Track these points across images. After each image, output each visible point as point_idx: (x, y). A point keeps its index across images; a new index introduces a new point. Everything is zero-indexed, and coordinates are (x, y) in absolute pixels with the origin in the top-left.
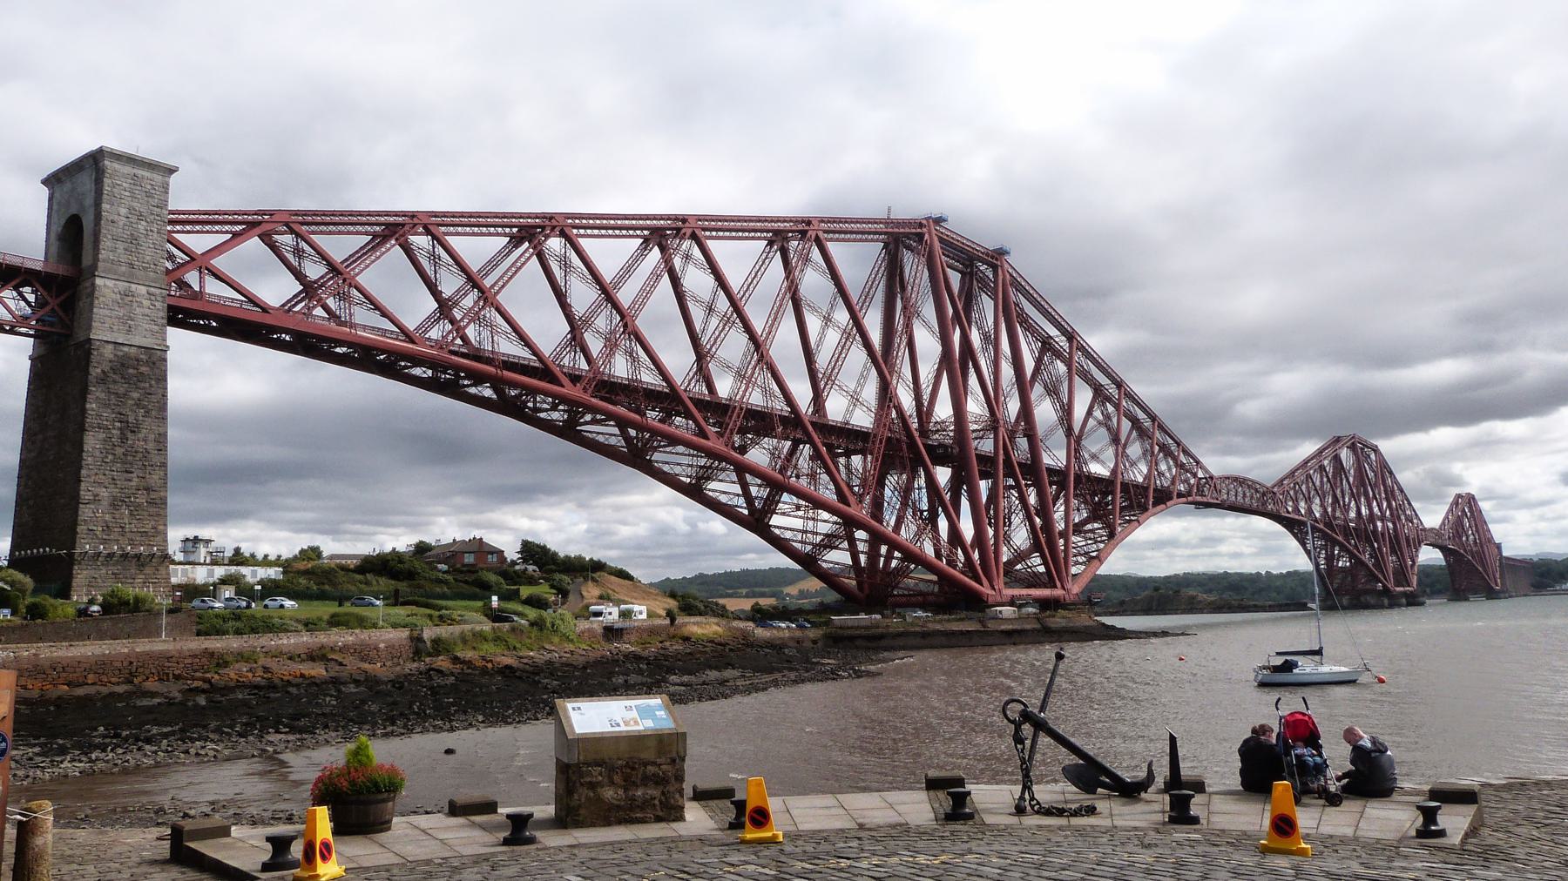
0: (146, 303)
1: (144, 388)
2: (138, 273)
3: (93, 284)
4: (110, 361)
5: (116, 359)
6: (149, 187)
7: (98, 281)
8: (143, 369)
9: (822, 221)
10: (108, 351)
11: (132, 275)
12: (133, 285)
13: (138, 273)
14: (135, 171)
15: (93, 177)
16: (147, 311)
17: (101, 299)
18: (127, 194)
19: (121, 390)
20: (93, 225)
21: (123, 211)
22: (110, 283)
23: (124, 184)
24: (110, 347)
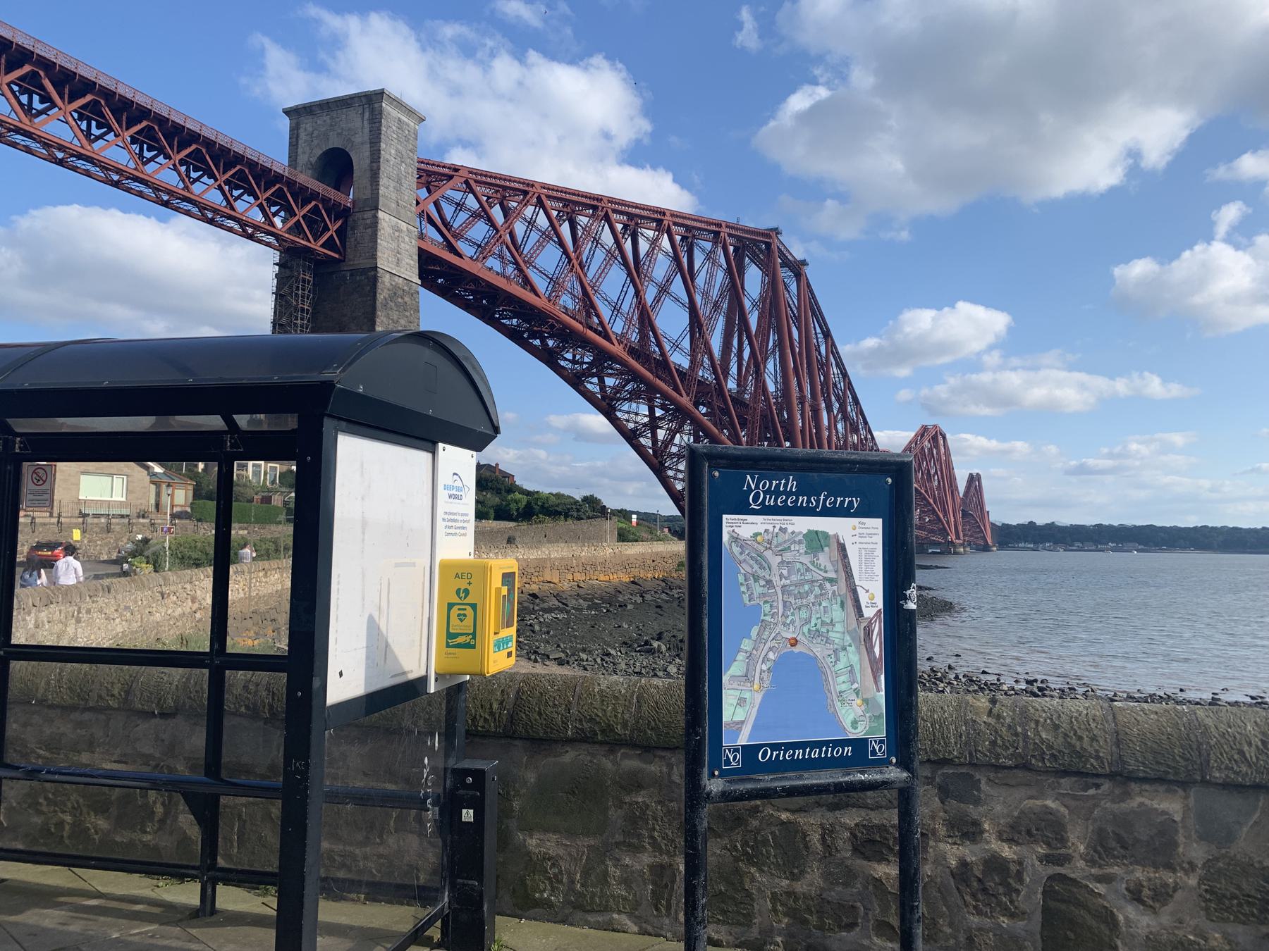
0: (407, 239)
1: (407, 317)
2: (402, 211)
3: (375, 217)
4: (389, 290)
5: (391, 287)
6: (407, 132)
7: (380, 214)
8: (407, 299)
9: (672, 215)
10: (387, 278)
11: (398, 212)
12: (400, 221)
13: (402, 211)
14: (399, 115)
15: (367, 115)
16: (408, 247)
17: (382, 232)
18: (395, 136)
19: (395, 317)
20: (368, 161)
21: (393, 152)
22: (387, 217)
23: (394, 128)
24: (388, 276)
